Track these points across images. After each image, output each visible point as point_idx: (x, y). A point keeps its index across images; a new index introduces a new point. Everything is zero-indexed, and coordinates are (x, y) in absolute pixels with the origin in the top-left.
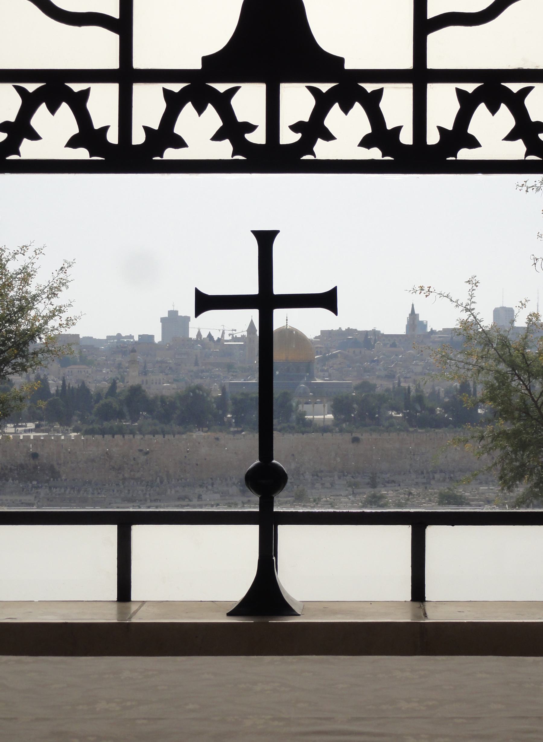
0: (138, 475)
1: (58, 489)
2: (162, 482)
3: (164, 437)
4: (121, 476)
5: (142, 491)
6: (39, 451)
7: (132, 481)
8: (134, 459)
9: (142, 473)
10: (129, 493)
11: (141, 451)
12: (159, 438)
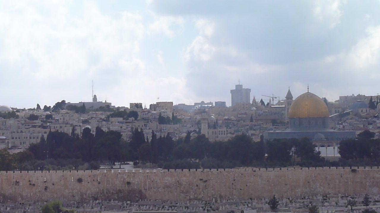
0: (200, 197)
1: (145, 207)
2: (216, 201)
3: (217, 170)
4: (188, 197)
5: (202, 207)
6: (131, 180)
7: (196, 201)
8: (197, 186)
9: (203, 195)
10: (193, 209)
11: (201, 180)
12: (214, 171)
